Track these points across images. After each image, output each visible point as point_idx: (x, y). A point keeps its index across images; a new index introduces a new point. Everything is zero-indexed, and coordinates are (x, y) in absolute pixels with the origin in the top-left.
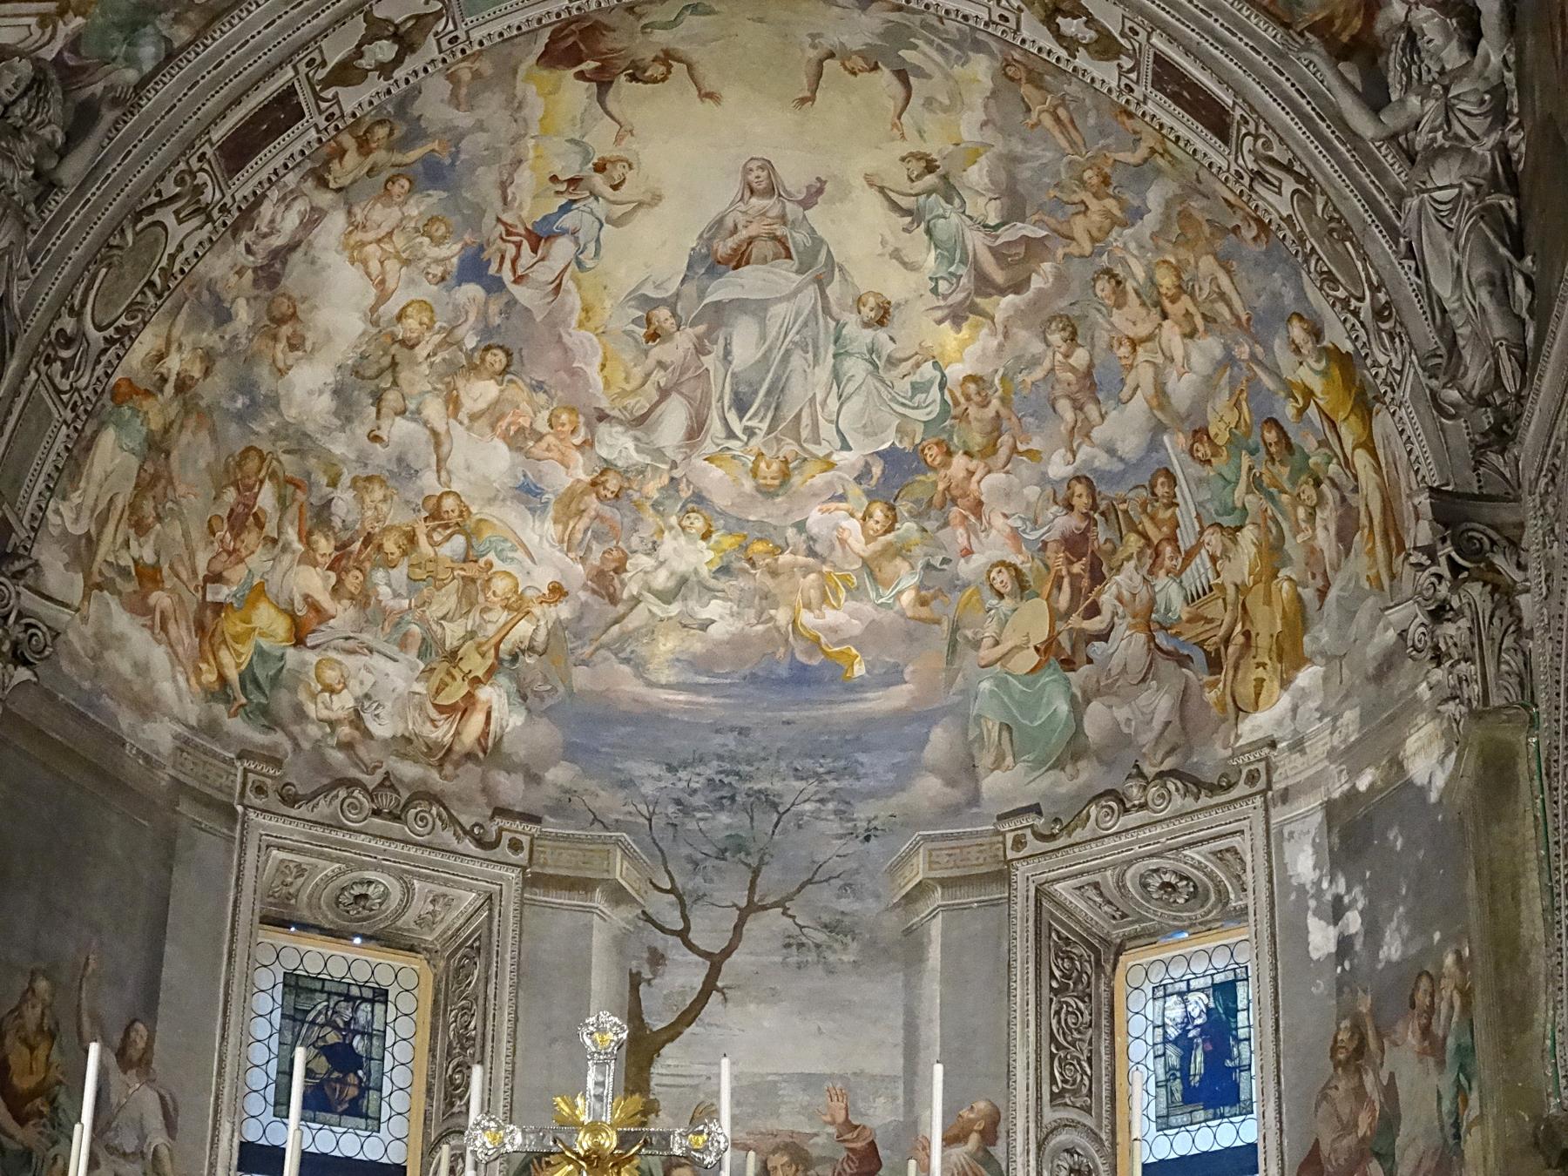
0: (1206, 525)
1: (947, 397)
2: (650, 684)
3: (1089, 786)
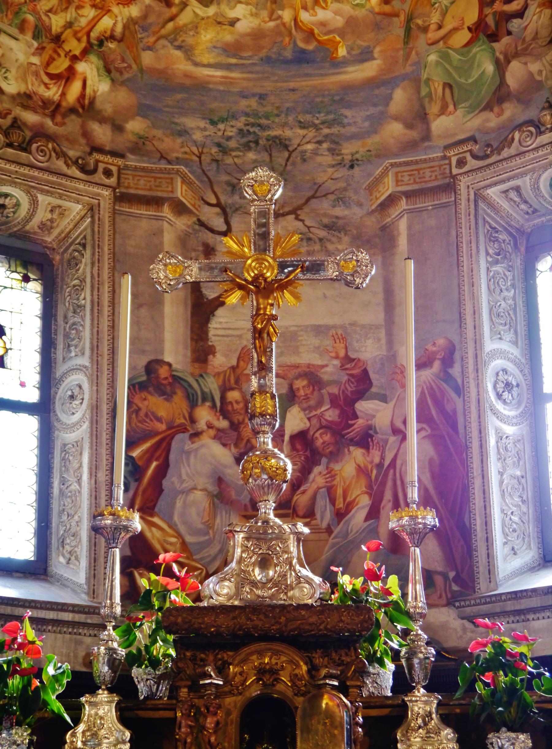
2: (196, 64)
3: (511, 120)
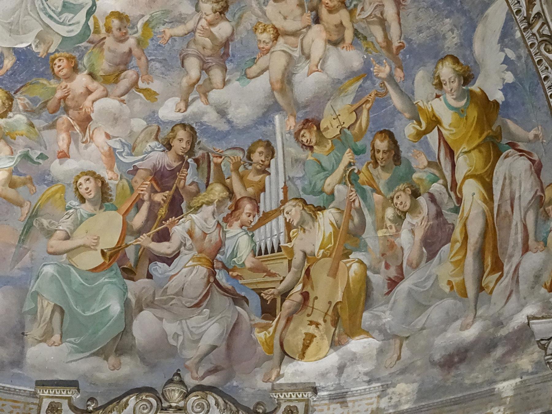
0: (290, 197)
1: (91, 23)
